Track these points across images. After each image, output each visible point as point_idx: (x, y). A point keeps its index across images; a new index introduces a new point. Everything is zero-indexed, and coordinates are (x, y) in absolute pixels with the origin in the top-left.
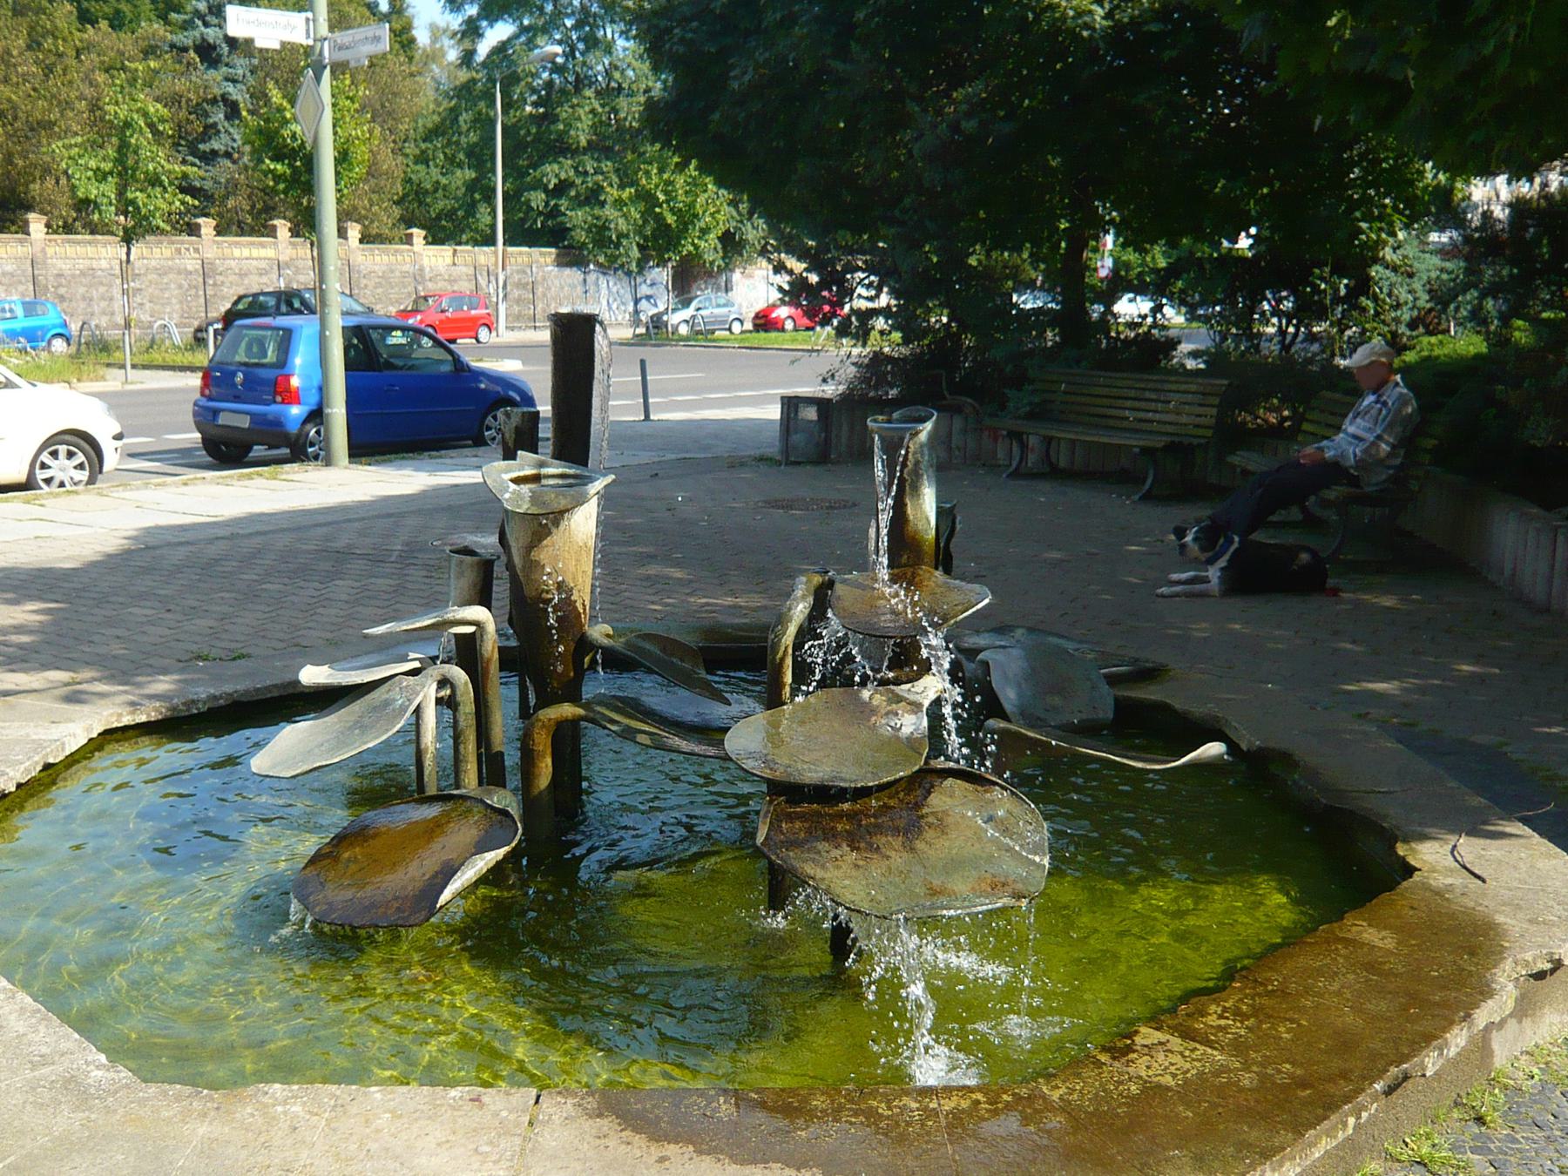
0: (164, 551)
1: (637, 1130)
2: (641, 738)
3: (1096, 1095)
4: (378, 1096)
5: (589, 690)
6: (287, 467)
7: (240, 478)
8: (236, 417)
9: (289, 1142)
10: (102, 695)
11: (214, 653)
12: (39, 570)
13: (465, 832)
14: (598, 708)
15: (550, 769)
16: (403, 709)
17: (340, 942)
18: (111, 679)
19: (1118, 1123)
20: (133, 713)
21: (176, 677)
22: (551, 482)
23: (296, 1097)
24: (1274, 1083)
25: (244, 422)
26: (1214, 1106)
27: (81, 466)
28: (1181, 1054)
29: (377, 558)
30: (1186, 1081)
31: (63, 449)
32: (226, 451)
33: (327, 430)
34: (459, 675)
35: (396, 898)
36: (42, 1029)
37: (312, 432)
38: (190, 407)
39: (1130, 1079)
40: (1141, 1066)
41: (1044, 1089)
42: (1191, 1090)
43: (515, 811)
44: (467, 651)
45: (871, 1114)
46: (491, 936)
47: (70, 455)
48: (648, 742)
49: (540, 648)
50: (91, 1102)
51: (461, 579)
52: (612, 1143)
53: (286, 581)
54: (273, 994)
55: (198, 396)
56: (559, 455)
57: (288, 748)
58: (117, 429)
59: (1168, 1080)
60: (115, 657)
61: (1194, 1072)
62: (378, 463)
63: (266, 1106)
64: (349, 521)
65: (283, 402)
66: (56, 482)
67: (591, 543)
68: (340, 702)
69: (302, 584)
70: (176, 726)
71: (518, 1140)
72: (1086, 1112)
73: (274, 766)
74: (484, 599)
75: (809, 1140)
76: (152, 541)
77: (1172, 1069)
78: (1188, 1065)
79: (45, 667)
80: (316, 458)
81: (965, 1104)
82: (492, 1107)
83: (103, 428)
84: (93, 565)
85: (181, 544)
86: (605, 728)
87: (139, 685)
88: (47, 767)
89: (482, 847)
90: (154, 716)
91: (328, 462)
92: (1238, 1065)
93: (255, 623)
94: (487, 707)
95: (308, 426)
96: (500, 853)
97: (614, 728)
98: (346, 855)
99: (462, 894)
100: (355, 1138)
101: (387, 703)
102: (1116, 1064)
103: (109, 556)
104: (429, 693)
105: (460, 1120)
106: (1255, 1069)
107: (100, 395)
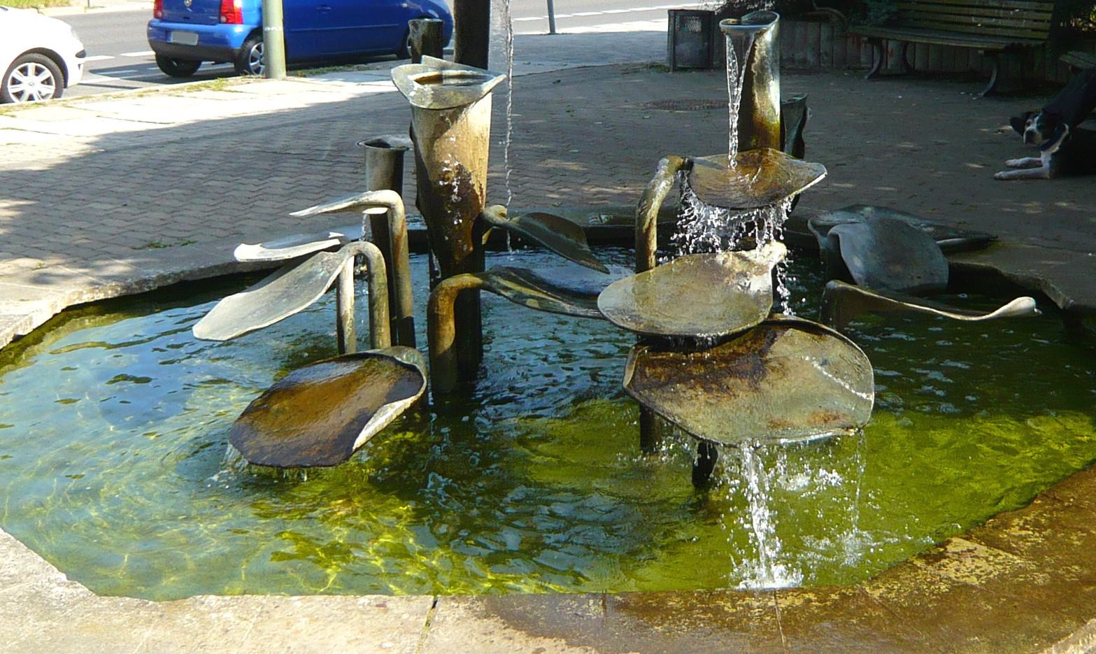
0: (121, 154)
1: (518, 627)
2: (530, 302)
3: (911, 593)
4: (299, 604)
5: (490, 262)
6: (231, 80)
7: (190, 90)
8: (186, 35)
9: (222, 642)
10: (65, 277)
11: (165, 241)
12: (11, 172)
13: (380, 385)
14: (494, 278)
15: (453, 331)
16: (325, 280)
17: (269, 481)
18: (73, 264)
19: (929, 616)
20: (92, 291)
21: (130, 261)
22: (452, 82)
23: (228, 606)
24: (1063, 581)
25: (194, 41)
26: (1011, 600)
27: (48, 81)
28: (986, 559)
29: (308, 158)
30: (989, 581)
31: (31, 67)
32: (177, 66)
33: (266, 47)
34: (373, 251)
35: (318, 443)
36: (11, 553)
37: (254, 49)
38: (145, 28)
39: (941, 581)
40: (951, 570)
41: (867, 589)
42: (992, 588)
43: (422, 367)
44: (381, 229)
45: (718, 611)
46: (399, 475)
47: (38, 71)
48: (537, 306)
49: (448, 230)
50: (52, 613)
51: (376, 168)
52: (496, 638)
53: (229, 178)
54: (214, 527)
55: (151, 18)
56: (462, 59)
57: (226, 316)
58: (80, 48)
59: (973, 581)
60: (77, 246)
61: (996, 573)
62: (312, 75)
63: (202, 613)
64: (286, 125)
65: (227, 22)
66: (26, 96)
67: (487, 134)
68: (269, 277)
69: (244, 180)
70: (128, 303)
71: (416, 638)
72: (901, 607)
73: (211, 332)
74: (396, 185)
75: (664, 633)
76: (111, 147)
77: (978, 571)
78: (991, 568)
79: (17, 255)
80: (257, 71)
81: (798, 602)
82: (396, 611)
83: (67, 47)
84: (59, 167)
85: (136, 148)
86: (499, 294)
87: (98, 268)
88: (17, 338)
89: (392, 398)
90: (111, 294)
91: (268, 75)
92: (1034, 567)
93: (200, 215)
94: (398, 278)
95: (250, 43)
96: (408, 402)
97: (508, 294)
98: (276, 407)
99: (376, 438)
100: (277, 638)
101: (310, 276)
102: (930, 568)
103: (73, 159)
104: (346, 267)
105: (368, 623)
106: (1048, 570)
107: (65, 19)
